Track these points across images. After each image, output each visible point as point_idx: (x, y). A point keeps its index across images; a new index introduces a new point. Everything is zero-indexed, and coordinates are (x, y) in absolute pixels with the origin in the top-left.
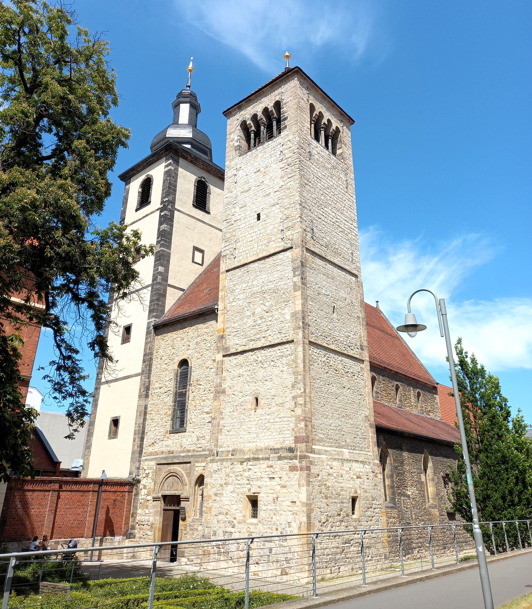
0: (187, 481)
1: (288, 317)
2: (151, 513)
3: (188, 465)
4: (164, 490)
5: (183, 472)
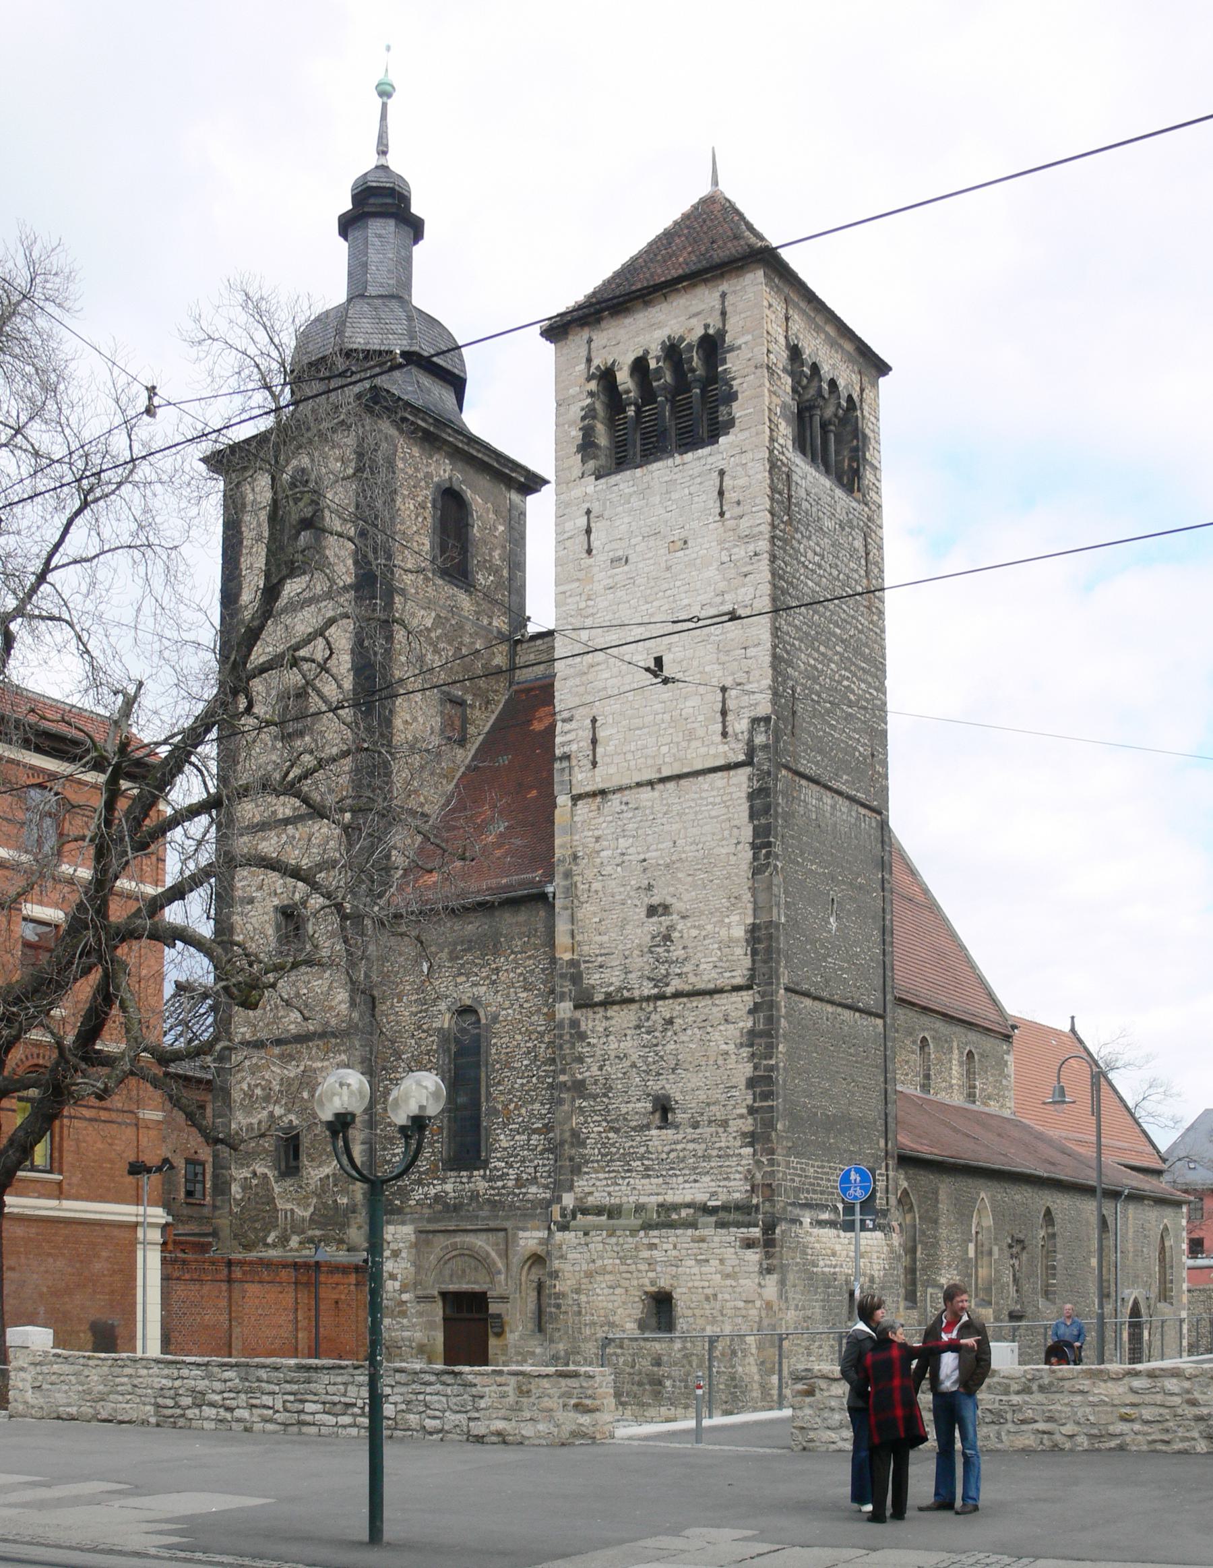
0: (500, 1265)
1: (739, 932)
2: (414, 1325)
3: (502, 1234)
4: (444, 1282)
5: (489, 1249)
